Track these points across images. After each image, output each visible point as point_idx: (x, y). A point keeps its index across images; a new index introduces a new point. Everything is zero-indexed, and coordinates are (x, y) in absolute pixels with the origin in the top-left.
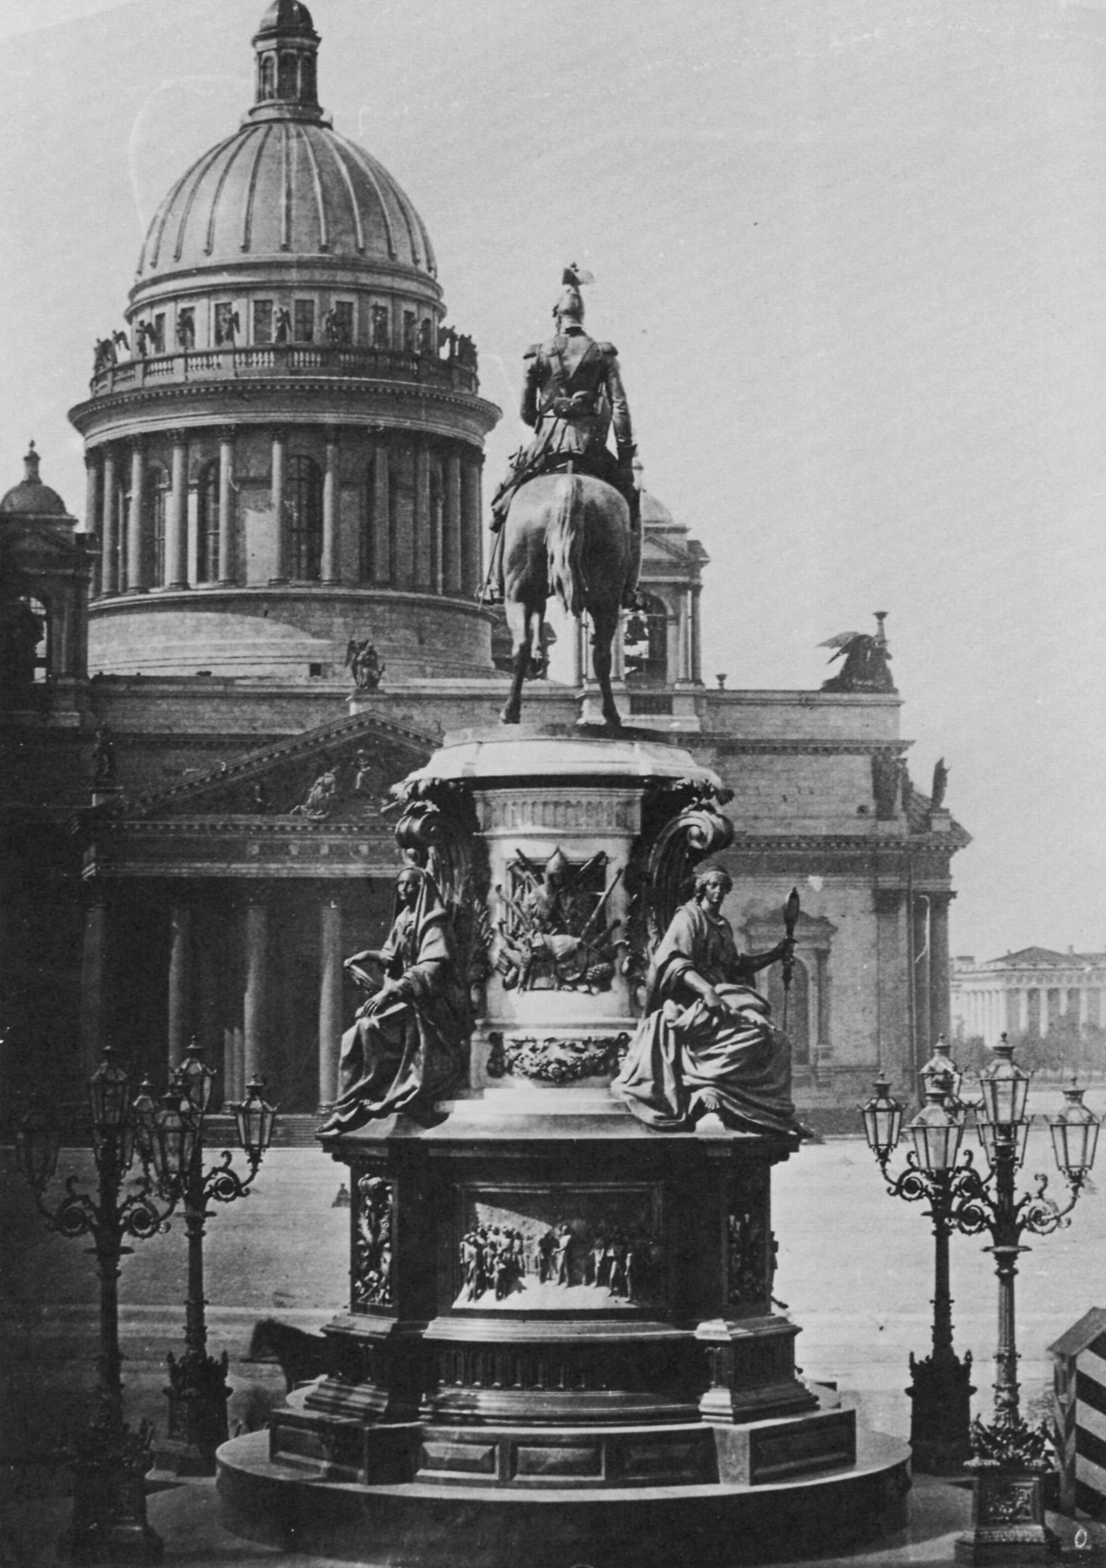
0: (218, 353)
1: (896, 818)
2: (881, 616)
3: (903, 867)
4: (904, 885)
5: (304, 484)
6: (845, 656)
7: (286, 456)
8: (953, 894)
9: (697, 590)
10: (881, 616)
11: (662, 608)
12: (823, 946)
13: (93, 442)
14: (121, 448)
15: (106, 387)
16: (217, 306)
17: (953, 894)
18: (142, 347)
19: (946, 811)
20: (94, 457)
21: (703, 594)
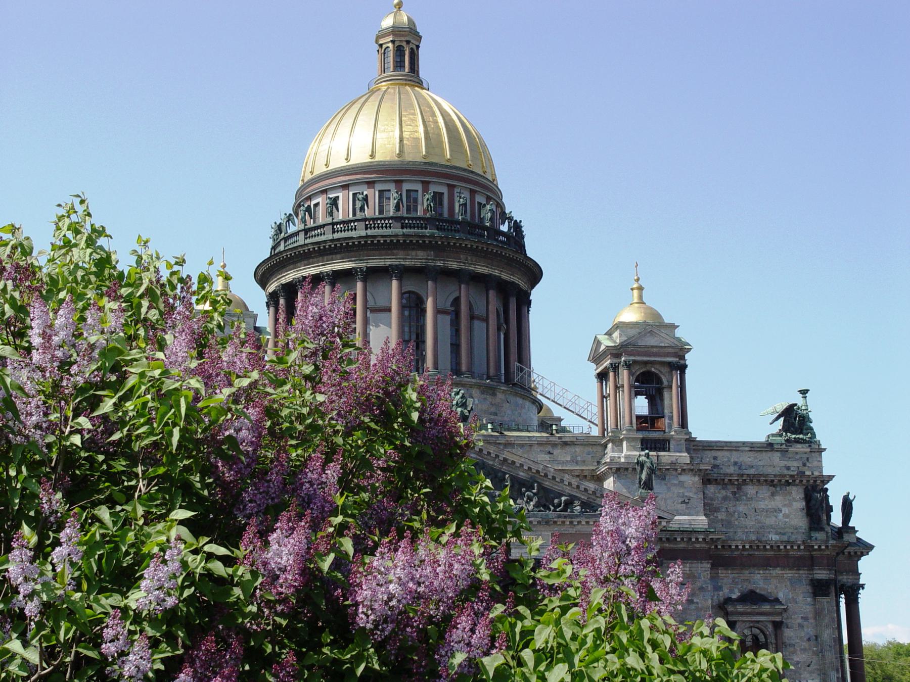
0: (354, 221)
1: (822, 529)
2: (804, 392)
3: (831, 563)
4: (833, 576)
5: (413, 307)
6: (782, 419)
7: (402, 294)
8: (862, 586)
9: (682, 368)
10: (804, 392)
11: (659, 381)
12: (778, 619)
13: (272, 288)
14: (290, 290)
15: (281, 248)
16: (354, 195)
17: (862, 586)
18: (304, 221)
19: (854, 528)
20: (273, 299)
21: (687, 371)
